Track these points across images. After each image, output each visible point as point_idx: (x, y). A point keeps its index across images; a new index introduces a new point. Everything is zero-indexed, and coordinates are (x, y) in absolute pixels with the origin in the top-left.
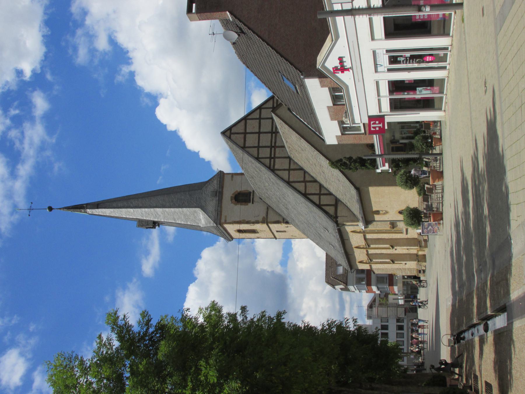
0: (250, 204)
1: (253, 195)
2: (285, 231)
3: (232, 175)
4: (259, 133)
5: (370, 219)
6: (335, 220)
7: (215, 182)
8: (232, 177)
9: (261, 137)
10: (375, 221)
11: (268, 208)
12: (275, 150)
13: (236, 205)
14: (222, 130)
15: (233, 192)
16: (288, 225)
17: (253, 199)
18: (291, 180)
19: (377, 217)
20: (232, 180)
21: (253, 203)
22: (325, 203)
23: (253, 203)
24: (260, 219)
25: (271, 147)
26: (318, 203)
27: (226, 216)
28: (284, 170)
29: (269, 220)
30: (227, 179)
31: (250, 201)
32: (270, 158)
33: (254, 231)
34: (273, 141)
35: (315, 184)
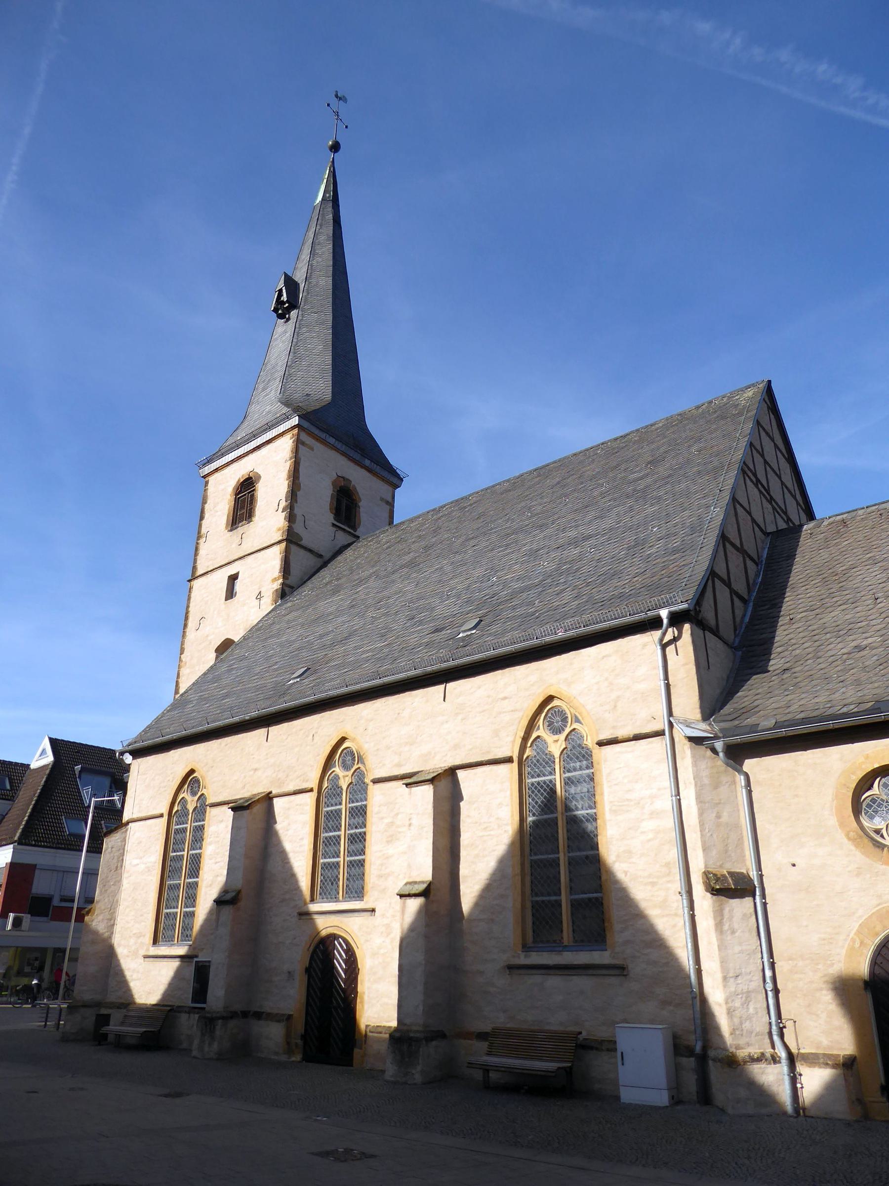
0: (330, 518)
2: (230, 593)
3: (391, 504)
8: (387, 503)
11: (320, 556)
13: (334, 483)
17: (344, 530)
20: (382, 499)
21: (334, 525)
24: (298, 528)
29: (294, 548)
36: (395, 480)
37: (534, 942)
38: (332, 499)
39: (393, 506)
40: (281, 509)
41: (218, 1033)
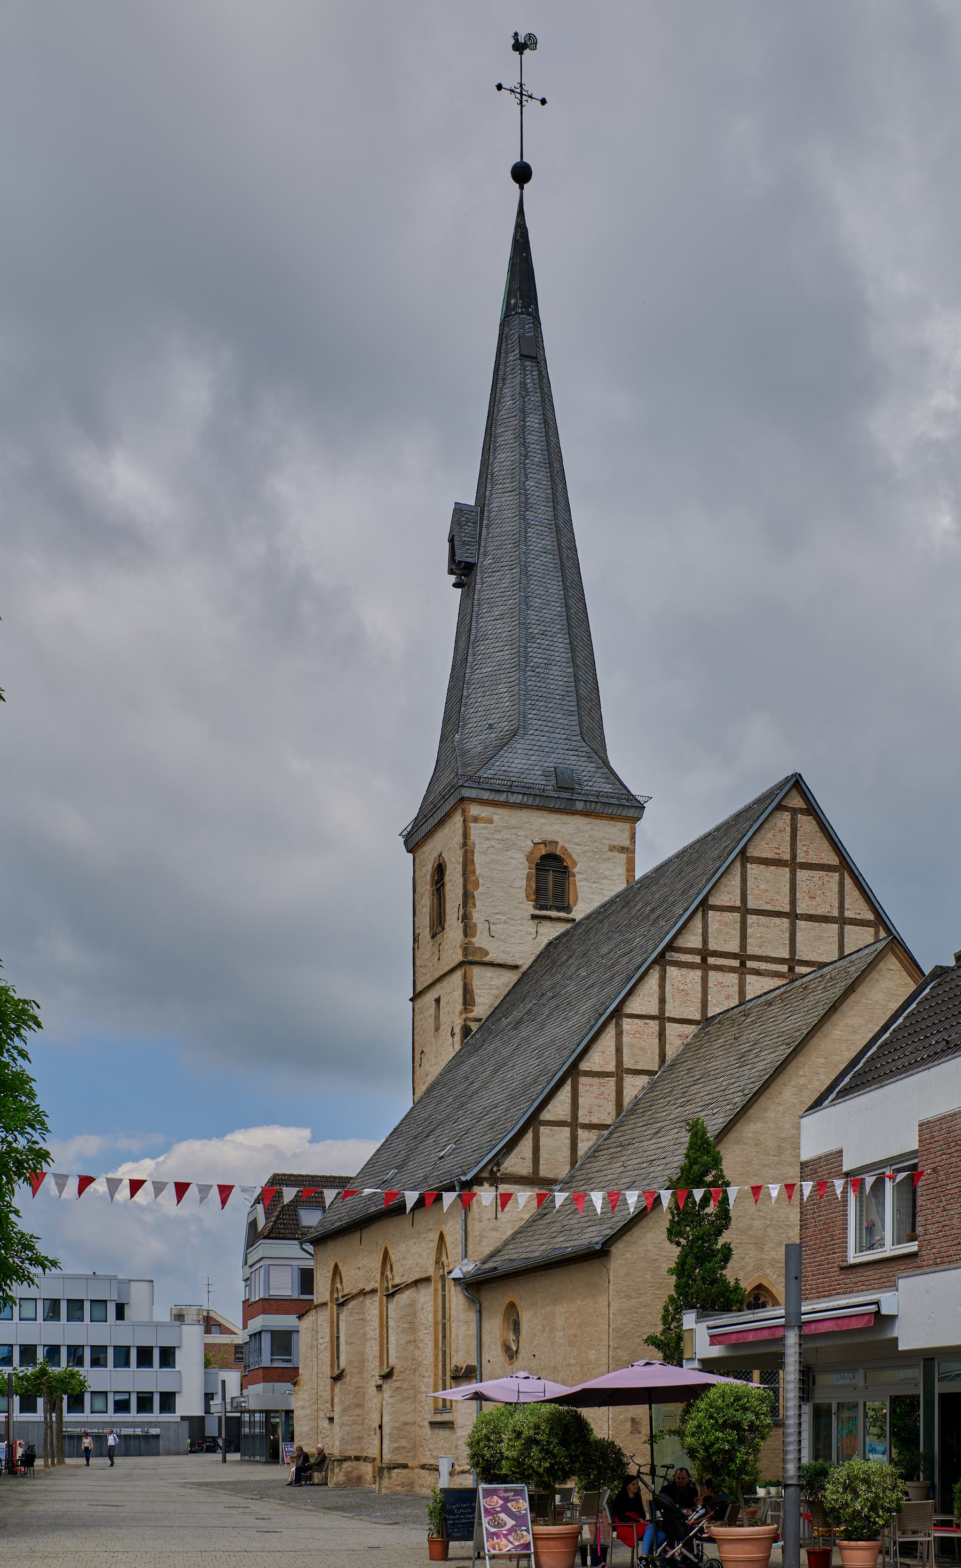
1: (559, 919)
3: (628, 851)
4: (793, 916)
6: (486, 1174)
7: (608, 788)
8: (623, 849)
9: (777, 920)
12: (732, 969)
14: (810, 781)
15: (570, 847)
16: (457, 1038)
18: (627, 1024)
19: (494, 1327)
20: (612, 848)
21: (534, 917)
22: (543, 1141)
23: (534, 917)
24: (480, 940)
25: (742, 957)
26: (546, 1116)
27: (490, 821)
28: (662, 1001)
30: (615, 832)
32: (705, 953)
34: (763, 966)
35: (611, 1107)
36: (631, 813)
38: (528, 880)
39: (633, 852)
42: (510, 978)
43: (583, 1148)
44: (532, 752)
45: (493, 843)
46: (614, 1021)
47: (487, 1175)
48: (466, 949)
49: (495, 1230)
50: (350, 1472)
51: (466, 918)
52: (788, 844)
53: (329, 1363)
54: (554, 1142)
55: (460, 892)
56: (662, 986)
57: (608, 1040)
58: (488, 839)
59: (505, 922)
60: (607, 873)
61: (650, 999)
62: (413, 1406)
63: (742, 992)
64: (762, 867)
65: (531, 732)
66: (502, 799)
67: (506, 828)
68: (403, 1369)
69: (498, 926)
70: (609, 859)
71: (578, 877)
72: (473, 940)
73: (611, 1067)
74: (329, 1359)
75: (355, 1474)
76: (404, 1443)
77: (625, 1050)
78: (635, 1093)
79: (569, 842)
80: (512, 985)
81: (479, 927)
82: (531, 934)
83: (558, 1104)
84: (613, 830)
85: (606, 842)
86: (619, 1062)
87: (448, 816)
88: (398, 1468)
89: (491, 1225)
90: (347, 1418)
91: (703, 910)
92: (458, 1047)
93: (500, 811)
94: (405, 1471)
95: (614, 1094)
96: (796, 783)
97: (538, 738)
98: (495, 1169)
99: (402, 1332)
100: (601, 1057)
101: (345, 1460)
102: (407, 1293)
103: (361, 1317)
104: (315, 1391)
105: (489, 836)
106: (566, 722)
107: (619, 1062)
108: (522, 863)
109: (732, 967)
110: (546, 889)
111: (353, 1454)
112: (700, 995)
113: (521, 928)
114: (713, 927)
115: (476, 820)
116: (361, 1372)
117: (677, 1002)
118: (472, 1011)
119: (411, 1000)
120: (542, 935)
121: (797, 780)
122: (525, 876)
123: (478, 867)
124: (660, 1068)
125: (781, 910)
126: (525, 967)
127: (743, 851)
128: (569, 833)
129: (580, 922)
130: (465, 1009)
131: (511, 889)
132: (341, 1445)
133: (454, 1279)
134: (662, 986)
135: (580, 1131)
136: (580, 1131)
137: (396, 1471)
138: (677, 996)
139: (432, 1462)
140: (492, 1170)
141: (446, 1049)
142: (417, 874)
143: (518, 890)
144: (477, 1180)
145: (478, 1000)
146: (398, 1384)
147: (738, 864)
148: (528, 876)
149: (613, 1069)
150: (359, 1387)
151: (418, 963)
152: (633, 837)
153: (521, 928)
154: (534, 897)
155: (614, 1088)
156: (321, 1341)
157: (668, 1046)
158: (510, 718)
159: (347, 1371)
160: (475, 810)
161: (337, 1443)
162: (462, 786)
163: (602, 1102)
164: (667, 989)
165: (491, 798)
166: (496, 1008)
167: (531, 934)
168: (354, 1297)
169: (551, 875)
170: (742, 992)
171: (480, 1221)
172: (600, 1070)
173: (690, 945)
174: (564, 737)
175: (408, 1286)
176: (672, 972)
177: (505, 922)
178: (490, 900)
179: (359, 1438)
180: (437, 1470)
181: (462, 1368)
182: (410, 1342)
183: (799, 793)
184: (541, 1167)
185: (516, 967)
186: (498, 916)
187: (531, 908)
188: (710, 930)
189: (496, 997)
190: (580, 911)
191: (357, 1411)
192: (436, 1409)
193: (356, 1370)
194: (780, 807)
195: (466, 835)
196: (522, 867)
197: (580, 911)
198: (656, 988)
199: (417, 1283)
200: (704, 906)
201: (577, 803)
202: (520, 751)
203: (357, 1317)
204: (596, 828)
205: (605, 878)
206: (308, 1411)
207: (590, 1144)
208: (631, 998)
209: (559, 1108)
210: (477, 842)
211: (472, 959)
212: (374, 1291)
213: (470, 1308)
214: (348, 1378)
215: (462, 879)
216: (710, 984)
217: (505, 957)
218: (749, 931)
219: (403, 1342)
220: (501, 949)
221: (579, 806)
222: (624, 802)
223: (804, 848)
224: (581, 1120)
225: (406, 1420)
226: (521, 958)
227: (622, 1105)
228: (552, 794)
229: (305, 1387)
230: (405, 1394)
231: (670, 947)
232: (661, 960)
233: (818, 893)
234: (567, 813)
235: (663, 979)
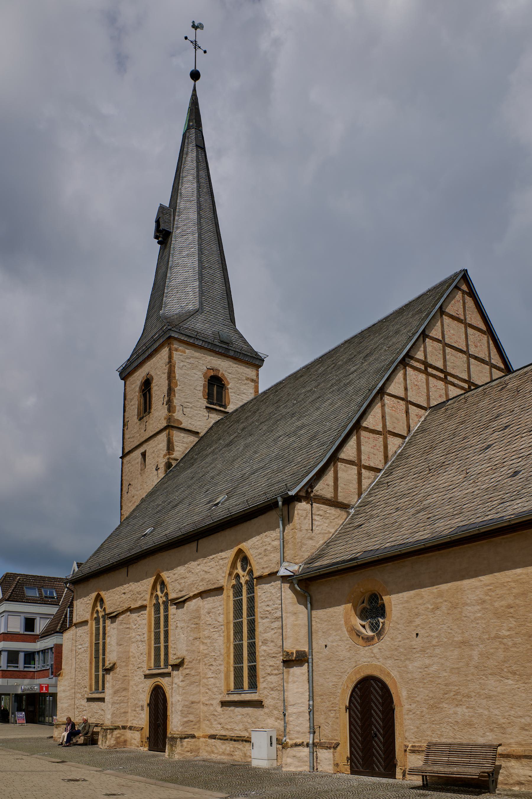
3: (255, 382)
5: (319, 591)
6: (303, 494)
8: (252, 380)
9: (460, 354)
10: (312, 609)
12: (440, 379)
13: (205, 375)
15: (226, 374)
20: (247, 379)
21: (207, 408)
23: (207, 408)
24: (178, 415)
26: (342, 455)
28: (406, 389)
31: (211, 404)
32: (427, 365)
33: (146, 407)
34: (456, 381)
35: (381, 457)
37: (235, 689)
38: (204, 387)
39: (258, 383)
40: (165, 403)
41: (109, 736)
42: (194, 440)
43: (365, 483)
44: (206, 322)
45: (185, 364)
46: (379, 396)
47: (304, 495)
48: (169, 419)
49: (311, 539)
50: (119, 737)
51: (169, 402)
52: (462, 310)
53: (88, 661)
54: (347, 474)
55: (165, 389)
56: (405, 379)
57: (377, 410)
58: (183, 361)
59: (191, 408)
60: (245, 391)
61: (399, 386)
62: (198, 689)
63: (447, 395)
64: (451, 319)
65: (205, 312)
66: (191, 341)
67: (193, 357)
68: (191, 660)
69: (188, 409)
70: (245, 384)
71: (230, 390)
72: (174, 414)
73: (379, 428)
74: (89, 658)
75: (122, 739)
76: (191, 717)
77: (387, 418)
78: (395, 449)
79: (226, 371)
80: (195, 443)
81: (177, 408)
82: (205, 416)
83: (349, 448)
84: (247, 369)
85: (244, 375)
86: (384, 426)
87: (156, 351)
88: (188, 738)
89: (309, 535)
90: (117, 698)
91: (423, 337)
92: (162, 475)
93: (189, 347)
94: (194, 740)
95: (382, 447)
96: (465, 276)
97: (209, 316)
98: (309, 490)
99: (191, 631)
100: (373, 420)
101: (116, 729)
102: (194, 601)
103: (128, 626)
104: (73, 680)
105: (184, 360)
106: (223, 311)
107: (384, 426)
108: (201, 378)
109: (440, 377)
110: (213, 395)
111: (120, 724)
112: (426, 391)
113: (200, 412)
114: (429, 349)
115: (176, 350)
116: (127, 666)
117: (414, 393)
118: (173, 454)
119: (121, 458)
120: (211, 418)
121: (464, 274)
122: (202, 385)
123: (177, 375)
124: (407, 434)
125: (462, 349)
126: (201, 435)
127: (441, 307)
128: (226, 367)
129: (233, 412)
130: (169, 452)
131: (195, 391)
132: (112, 718)
133: (282, 577)
134: (405, 379)
135: (363, 471)
136: (363, 471)
137: (186, 740)
138: (414, 388)
139: (246, 734)
140: (307, 491)
141: (153, 478)
142: (127, 390)
143: (199, 392)
144: (297, 498)
145: (176, 448)
146: (187, 671)
147: (439, 314)
148: (204, 385)
149: (381, 430)
150: (125, 676)
151: (127, 436)
152: (258, 375)
153: (200, 412)
154: (207, 397)
155: (382, 443)
156: (80, 647)
157: (411, 421)
158: (194, 304)
159: (118, 664)
160: (175, 345)
161: (109, 717)
162: (170, 329)
163: (376, 452)
164: (408, 382)
165: (186, 339)
166: (186, 455)
167: (205, 416)
168: (123, 612)
169: (215, 386)
170: (447, 395)
171: (301, 531)
172: (373, 428)
173: (417, 356)
174: (222, 318)
175: (195, 596)
176: (409, 370)
177: (191, 408)
178: (184, 394)
179: (125, 713)
180: (248, 740)
181: (292, 653)
182: (196, 639)
183: (465, 282)
184: (339, 494)
185: (197, 433)
186: (188, 404)
187: (205, 402)
188: (428, 351)
189: (186, 448)
190: (231, 408)
191: (124, 693)
192: (229, 691)
193: (124, 664)
194: (457, 287)
195: (170, 357)
196: (201, 379)
197: (231, 408)
198: (402, 379)
199: (202, 594)
200: (424, 335)
201: (231, 351)
202: (199, 320)
203: (125, 626)
204: (239, 366)
205: (244, 393)
206: (68, 694)
207: (370, 481)
208: (388, 382)
209: (349, 451)
210: (177, 362)
211: (171, 426)
212: (143, 608)
213: (299, 603)
214: (118, 669)
215: (167, 382)
216: (431, 385)
217: (191, 426)
218: (447, 357)
219: (191, 638)
220: (189, 422)
221: (232, 353)
222: (254, 356)
223: (470, 316)
224: (363, 463)
225: (193, 700)
226: (200, 428)
227: (387, 457)
228: (218, 344)
229: (66, 678)
230: (193, 679)
231: (408, 355)
232: (404, 363)
233: (480, 345)
234: (225, 356)
235: (405, 374)
